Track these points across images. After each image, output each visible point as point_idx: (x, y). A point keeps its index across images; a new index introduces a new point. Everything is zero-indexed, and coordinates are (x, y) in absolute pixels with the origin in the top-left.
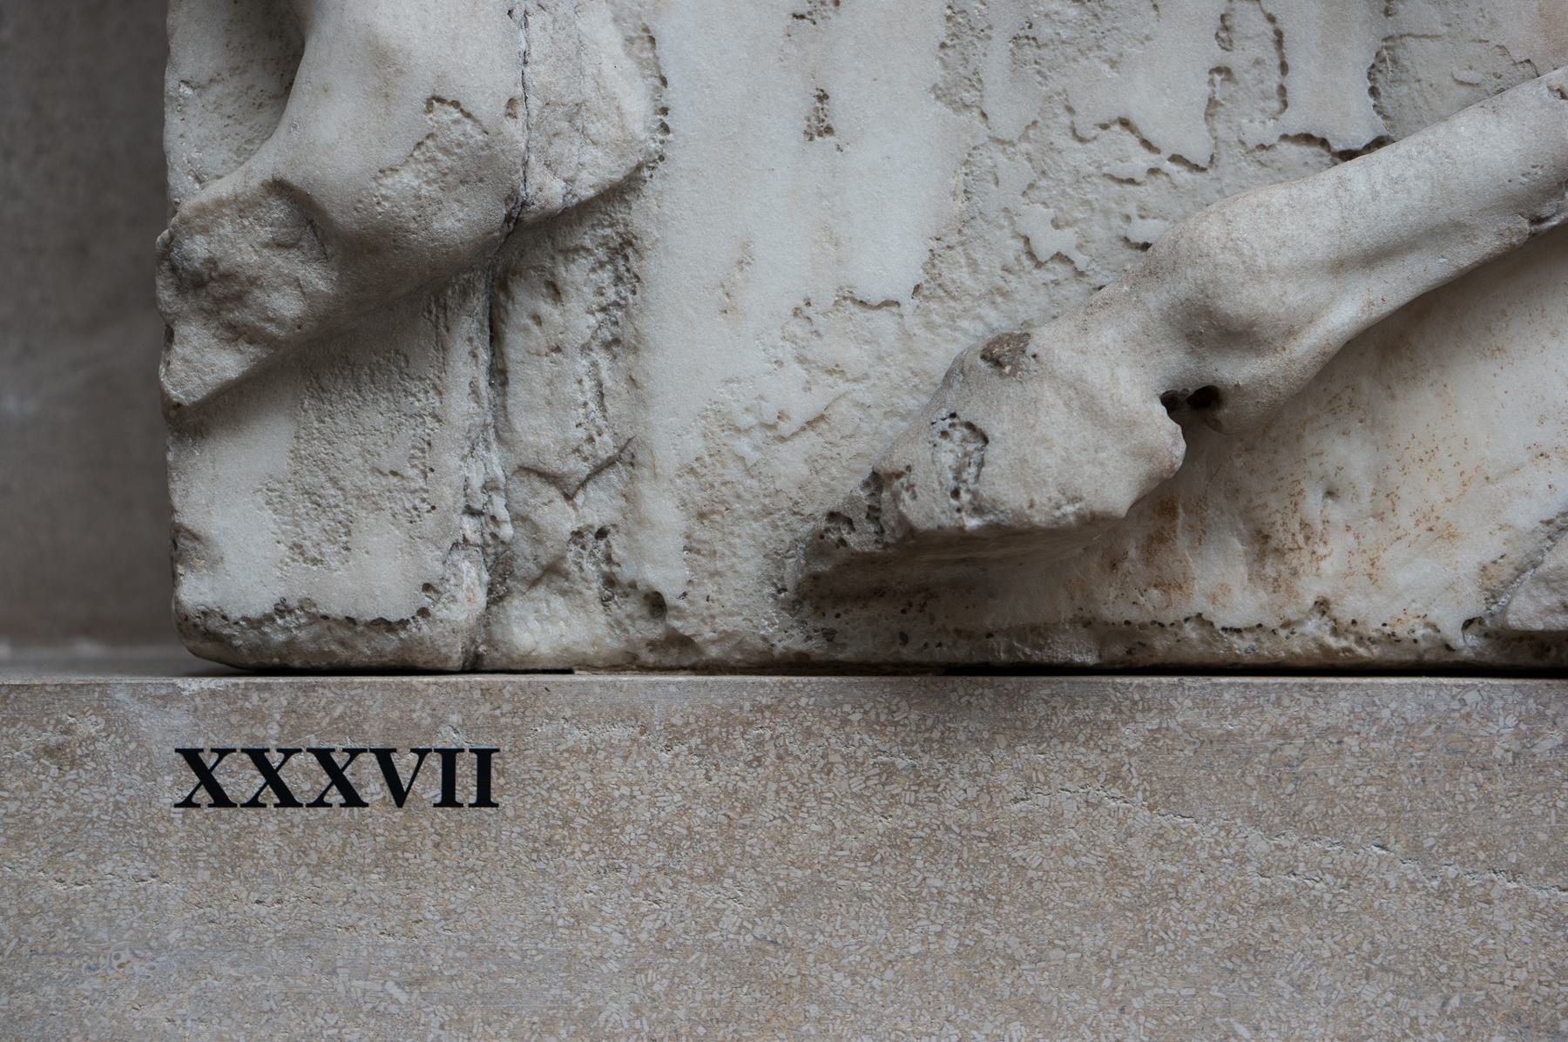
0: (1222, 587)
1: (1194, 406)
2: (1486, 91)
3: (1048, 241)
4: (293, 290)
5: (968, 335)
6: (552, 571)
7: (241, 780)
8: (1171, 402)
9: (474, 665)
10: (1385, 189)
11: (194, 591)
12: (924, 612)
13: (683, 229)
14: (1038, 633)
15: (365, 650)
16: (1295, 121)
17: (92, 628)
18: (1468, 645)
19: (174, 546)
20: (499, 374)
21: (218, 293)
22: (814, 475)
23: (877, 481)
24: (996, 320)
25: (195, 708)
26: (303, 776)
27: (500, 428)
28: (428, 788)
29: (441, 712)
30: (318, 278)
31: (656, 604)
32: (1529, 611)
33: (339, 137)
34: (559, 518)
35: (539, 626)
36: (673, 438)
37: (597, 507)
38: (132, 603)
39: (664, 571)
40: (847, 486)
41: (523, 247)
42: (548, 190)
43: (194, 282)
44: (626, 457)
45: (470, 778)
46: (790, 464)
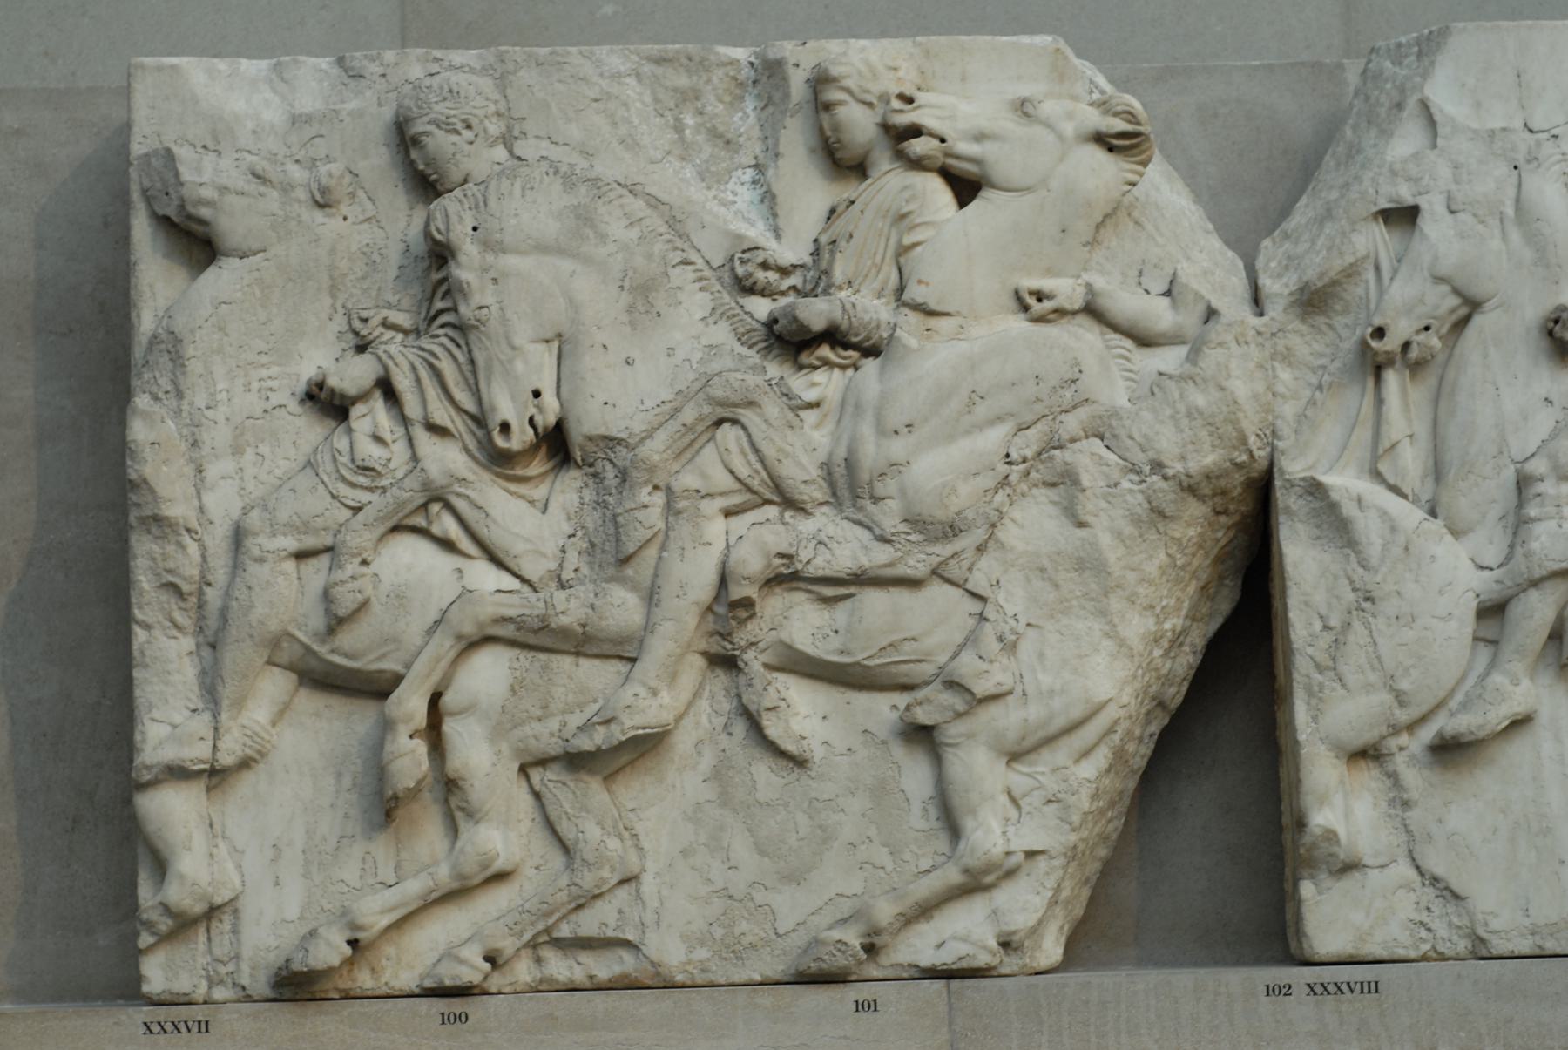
0: (364, 980)
1: (353, 943)
2: (417, 873)
3: (327, 907)
4: (165, 924)
5: (310, 927)
6: (221, 982)
7: (155, 1028)
8: (349, 943)
9: (205, 1002)
10: (390, 896)
11: (145, 988)
12: (296, 986)
13: (248, 908)
14: (326, 991)
15: (182, 1000)
16: (379, 879)
17: (122, 997)
18: (417, 991)
19: (138, 979)
20: (209, 939)
21: (149, 926)
22: (274, 959)
23: (288, 961)
24: (315, 924)
25: (145, 1013)
26: (169, 1027)
27: (210, 951)
28: (195, 1029)
29: (198, 1013)
30: (170, 922)
31: (244, 988)
32: (429, 983)
33: (175, 894)
34: (223, 970)
35: (219, 994)
36: (247, 952)
37: (231, 967)
38: (129, 990)
39: (245, 981)
40: (281, 962)
41: (212, 912)
42: (218, 900)
43: (144, 923)
44: (237, 957)
45: (204, 1026)
46: (272, 956)
